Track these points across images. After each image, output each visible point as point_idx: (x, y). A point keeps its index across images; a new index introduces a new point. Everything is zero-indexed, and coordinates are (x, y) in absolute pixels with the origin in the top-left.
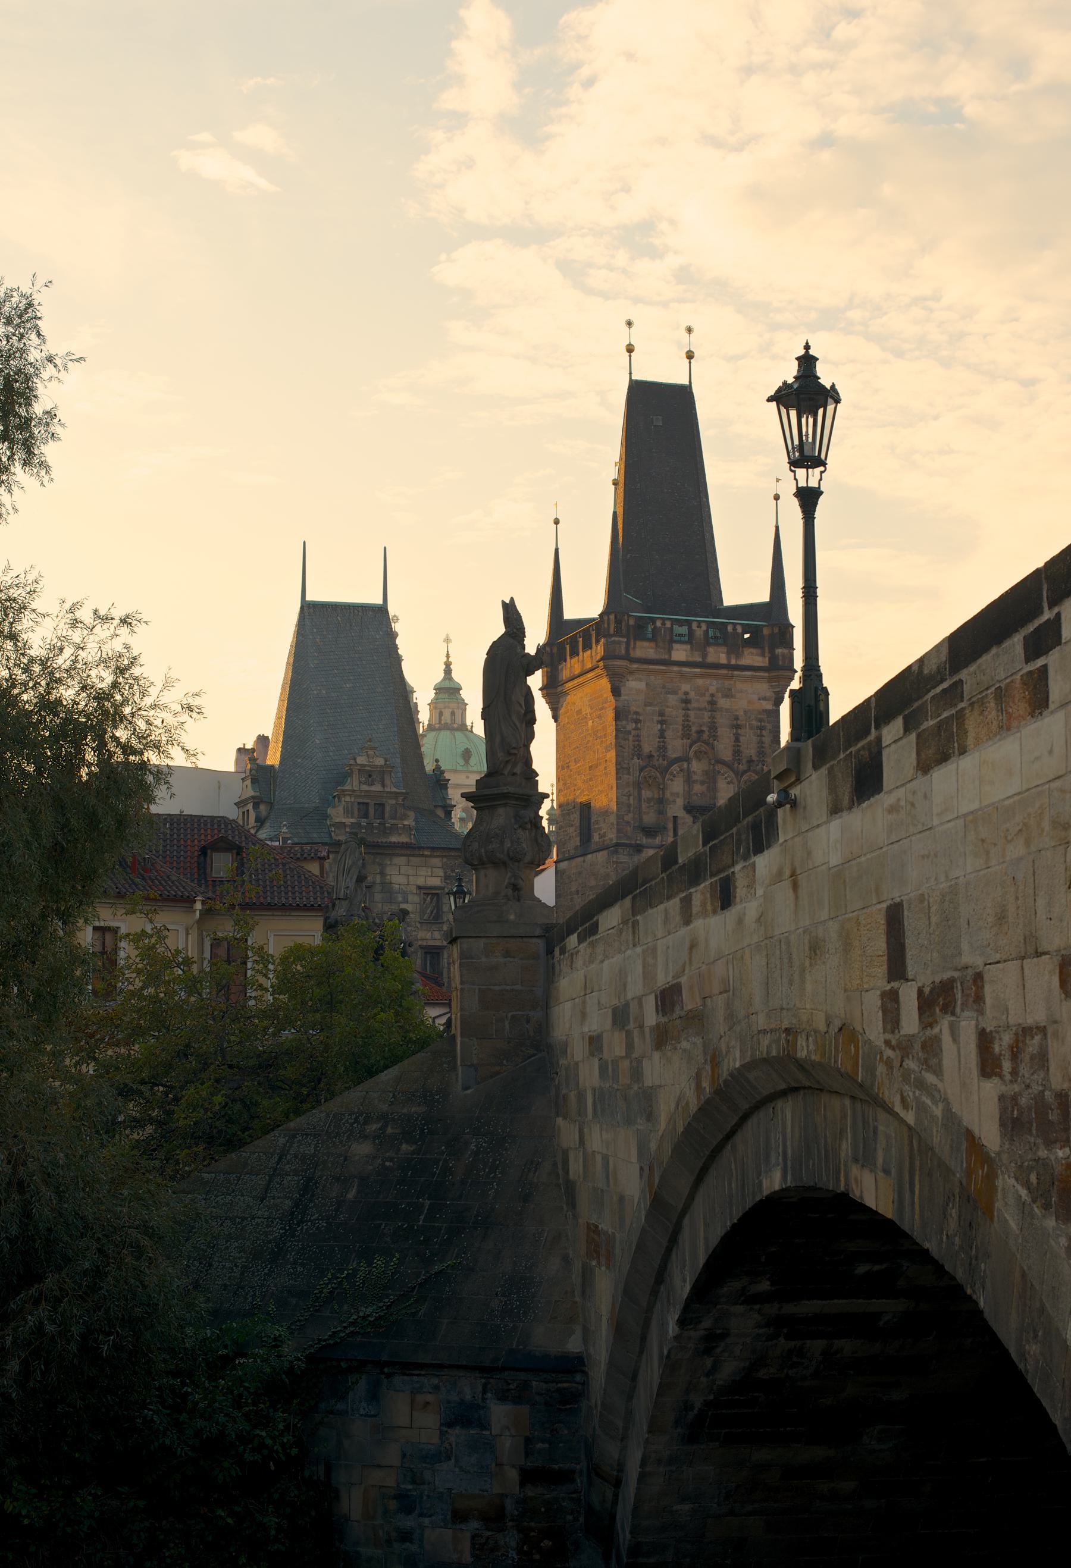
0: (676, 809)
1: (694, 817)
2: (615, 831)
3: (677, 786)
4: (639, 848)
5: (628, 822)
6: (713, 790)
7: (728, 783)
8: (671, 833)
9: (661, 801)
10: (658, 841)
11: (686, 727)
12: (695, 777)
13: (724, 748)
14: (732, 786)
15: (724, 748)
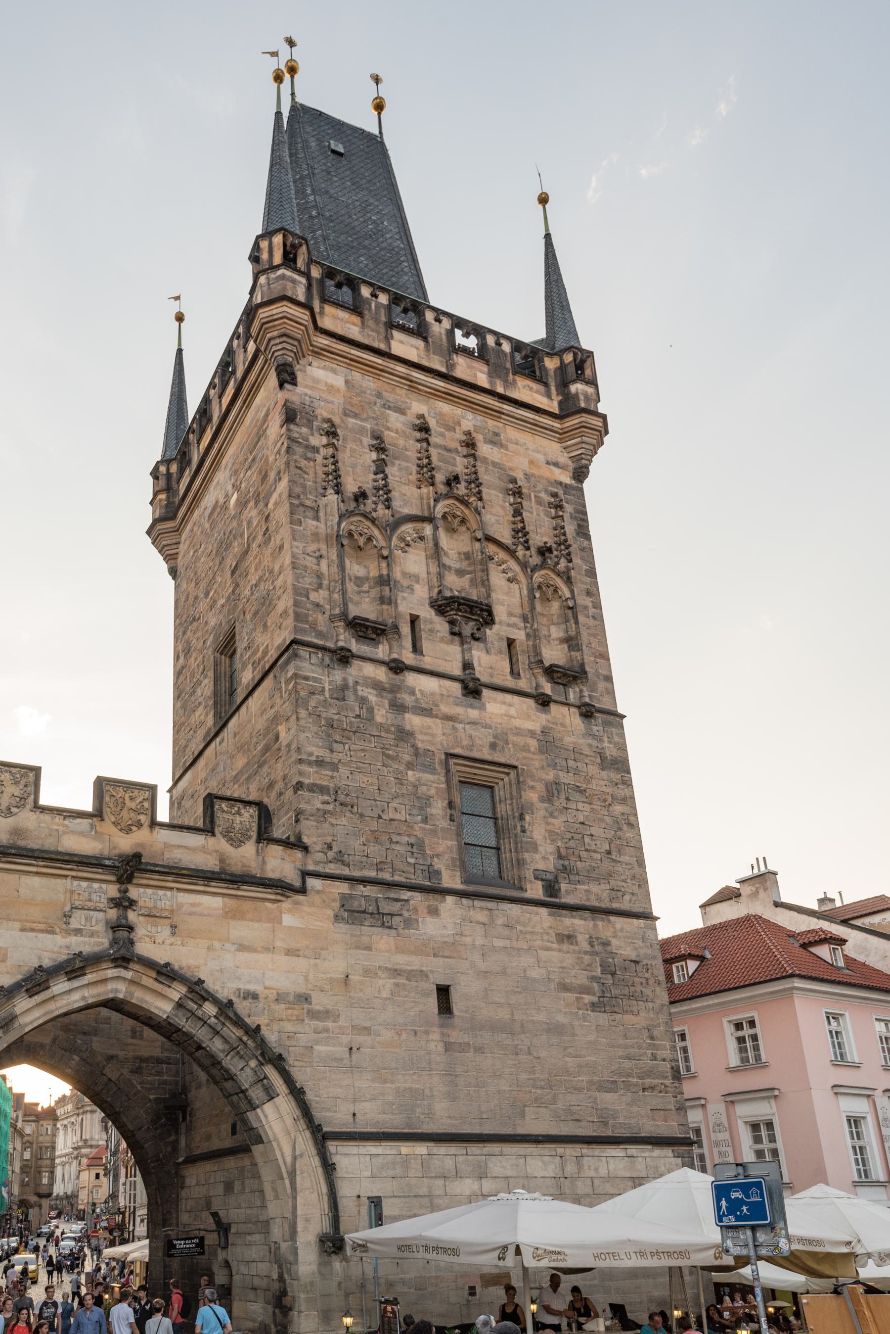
0: (415, 601)
1: (452, 623)
2: (290, 622)
3: (413, 563)
4: (344, 657)
5: (318, 605)
6: (486, 583)
7: (509, 580)
8: (408, 643)
9: (384, 581)
10: (382, 651)
11: (426, 471)
12: (446, 560)
13: (497, 518)
14: (515, 586)
15: (497, 518)
